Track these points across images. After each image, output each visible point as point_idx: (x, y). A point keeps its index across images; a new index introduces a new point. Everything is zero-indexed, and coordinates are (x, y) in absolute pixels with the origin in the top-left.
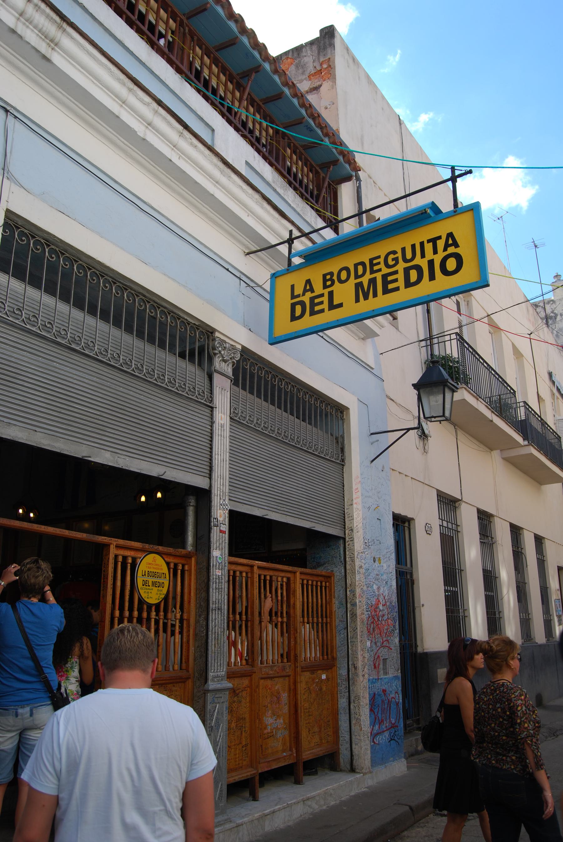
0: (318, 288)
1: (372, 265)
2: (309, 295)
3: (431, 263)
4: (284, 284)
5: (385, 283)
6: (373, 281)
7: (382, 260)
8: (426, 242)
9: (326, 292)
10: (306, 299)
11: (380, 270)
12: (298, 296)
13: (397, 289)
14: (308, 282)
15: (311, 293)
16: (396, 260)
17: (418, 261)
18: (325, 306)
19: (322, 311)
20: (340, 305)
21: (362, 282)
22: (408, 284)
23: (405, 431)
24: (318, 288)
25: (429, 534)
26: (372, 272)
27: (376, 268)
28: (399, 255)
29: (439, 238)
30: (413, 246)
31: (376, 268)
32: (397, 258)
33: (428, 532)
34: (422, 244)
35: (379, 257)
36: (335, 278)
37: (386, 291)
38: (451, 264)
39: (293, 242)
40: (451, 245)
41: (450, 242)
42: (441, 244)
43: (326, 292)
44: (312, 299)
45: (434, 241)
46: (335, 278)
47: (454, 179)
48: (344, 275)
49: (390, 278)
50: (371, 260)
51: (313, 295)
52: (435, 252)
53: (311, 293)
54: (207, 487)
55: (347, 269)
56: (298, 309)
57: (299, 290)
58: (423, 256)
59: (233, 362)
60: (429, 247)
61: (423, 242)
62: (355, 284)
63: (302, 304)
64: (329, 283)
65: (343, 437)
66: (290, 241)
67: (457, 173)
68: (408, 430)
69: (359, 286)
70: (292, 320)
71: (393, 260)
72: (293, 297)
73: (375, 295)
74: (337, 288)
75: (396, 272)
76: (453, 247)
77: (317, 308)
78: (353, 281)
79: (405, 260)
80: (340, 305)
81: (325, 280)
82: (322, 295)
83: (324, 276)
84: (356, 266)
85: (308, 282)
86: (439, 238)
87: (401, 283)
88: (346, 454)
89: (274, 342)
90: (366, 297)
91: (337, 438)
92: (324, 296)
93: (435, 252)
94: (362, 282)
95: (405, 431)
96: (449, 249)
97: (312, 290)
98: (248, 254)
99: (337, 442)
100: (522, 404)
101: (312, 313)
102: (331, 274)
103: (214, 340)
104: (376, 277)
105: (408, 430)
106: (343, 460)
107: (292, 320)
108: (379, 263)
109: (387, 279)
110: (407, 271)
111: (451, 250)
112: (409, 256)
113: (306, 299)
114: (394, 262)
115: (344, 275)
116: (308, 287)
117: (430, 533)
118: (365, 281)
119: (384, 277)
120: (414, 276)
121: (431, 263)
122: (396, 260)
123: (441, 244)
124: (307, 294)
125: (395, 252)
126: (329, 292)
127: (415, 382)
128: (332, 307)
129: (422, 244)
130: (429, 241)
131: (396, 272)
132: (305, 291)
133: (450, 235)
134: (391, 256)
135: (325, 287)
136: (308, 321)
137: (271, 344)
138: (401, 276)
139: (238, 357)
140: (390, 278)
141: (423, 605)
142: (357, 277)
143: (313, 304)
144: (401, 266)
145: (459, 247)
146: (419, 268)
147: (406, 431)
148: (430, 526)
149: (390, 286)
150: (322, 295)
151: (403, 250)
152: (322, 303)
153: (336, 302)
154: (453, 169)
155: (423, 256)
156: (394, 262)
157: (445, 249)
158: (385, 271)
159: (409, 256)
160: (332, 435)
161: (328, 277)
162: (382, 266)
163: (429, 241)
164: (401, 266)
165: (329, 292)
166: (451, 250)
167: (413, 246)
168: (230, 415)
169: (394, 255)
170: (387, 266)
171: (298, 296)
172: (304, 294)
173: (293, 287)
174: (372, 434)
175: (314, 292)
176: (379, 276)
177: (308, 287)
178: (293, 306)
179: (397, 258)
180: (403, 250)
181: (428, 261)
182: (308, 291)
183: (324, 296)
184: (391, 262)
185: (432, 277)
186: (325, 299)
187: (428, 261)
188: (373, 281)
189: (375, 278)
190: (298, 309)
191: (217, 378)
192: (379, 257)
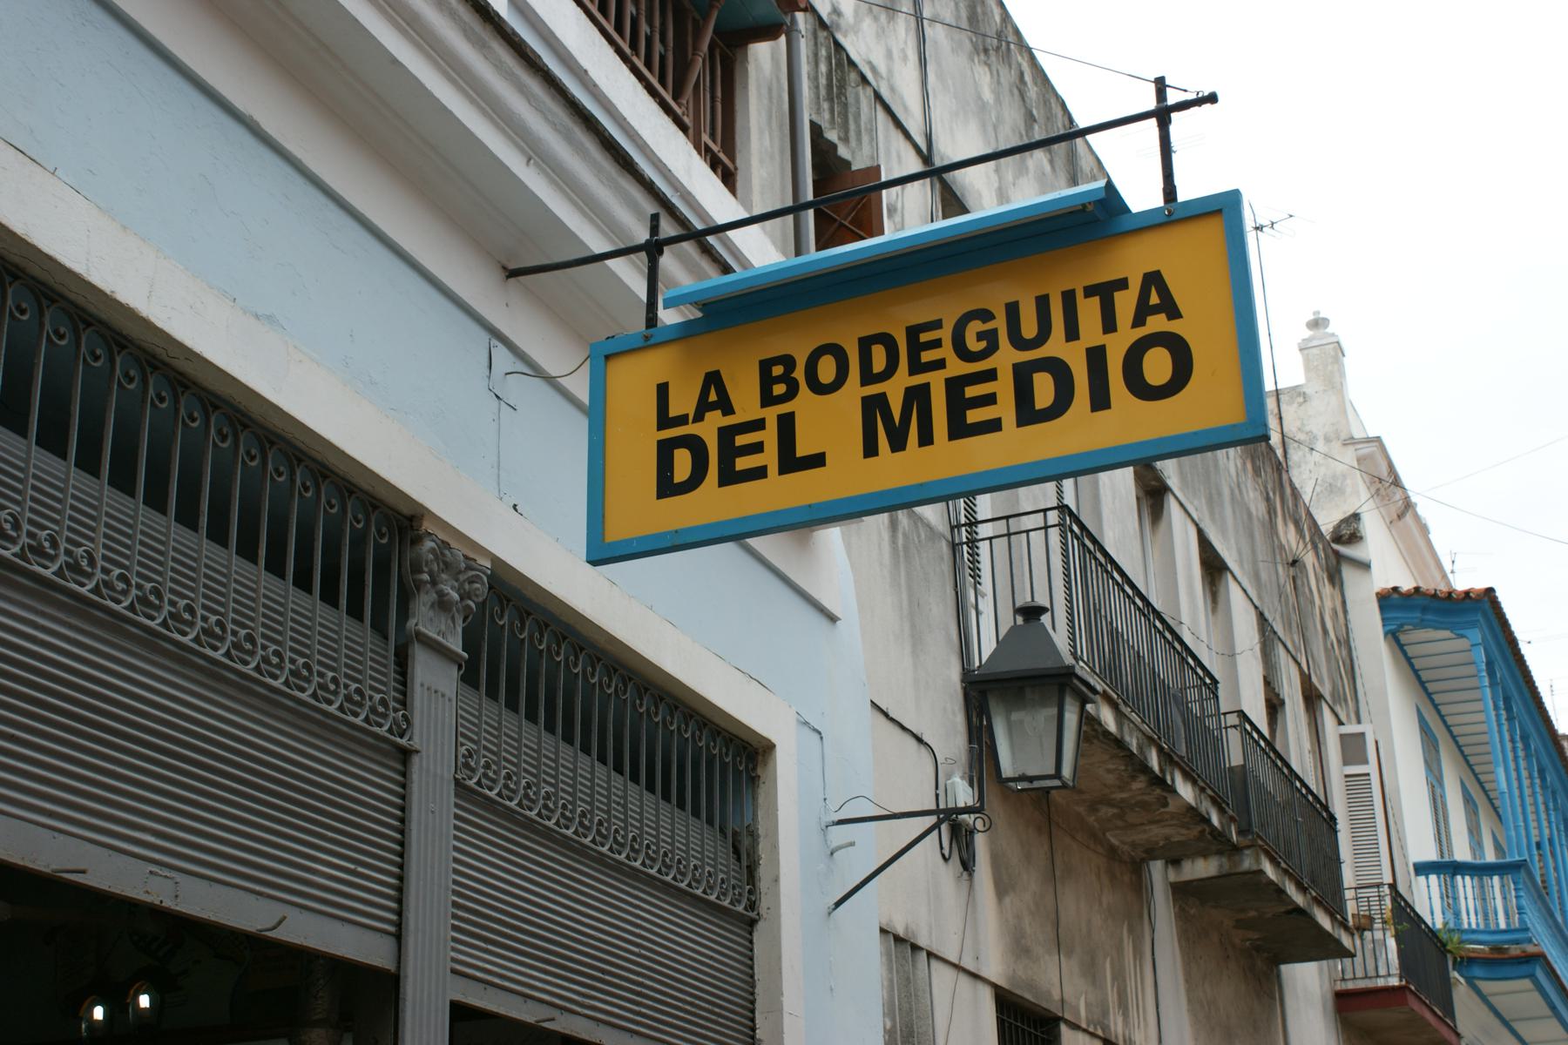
0: (747, 403)
1: (915, 347)
2: (715, 420)
3: (1096, 357)
5: (958, 404)
6: (918, 397)
7: (945, 334)
8: (1080, 294)
9: (771, 415)
10: (708, 429)
11: (940, 364)
12: (682, 420)
13: (994, 426)
14: (713, 379)
15: (725, 414)
16: (990, 337)
17: (1056, 346)
18: (770, 458)
19: (760, 473)
20: (817, 460)
21: (883, 395)
22: (1028, 414)
24: (747, 403)
26: (916, 367)
27: (927, 356)
28: (1000, 324)
29: (1122, 284)
31: (927, 356)
32: (995, 331)
34: (1069, 298)
35: (937, 325)
36: (799, 374)
37: (959, 429)
38: (1158, 366)
39: (661, 252)
40: (1156, 310)
41: (1154, 299)
42: (1125, 303)
43: (771, 415)
44: (726, 435)
45: (1105, 292)
46: (799, 374)
47: (1163, 115)
48: (827, 370)
49: (971, 392)
50: (913, 332)
52: (1109, 325)
53: (725, 414)
56: (683, 463)
58: (1072, 333)
59: (468, 607)
60: (1090, 311)
61: (1073, 291)
63: (696, 446)
64: (779, 389)
65: (753, 834)
66: (654, 249)
67: (1173, 98)
69: (874, 407)
70: (661, 494)
72: (664, 421)
73: (926, 439)
74: (805, 405)
75: (991, 375)
76: (1163, 316)
77: (742, 463)
78: (854, 391)
79: (1019, 342)
80: (817, 460)
81: (767, 381)
82: (759, 425)
83: (765, 366)
84: (865, 344)
85: (713, 379)
86: (1122, 284)
87: (1005, 408)
89: (601, 555)
90: (898, 444)
92: (763, 428)
93: (1109, 325)
94: (883, 395)
96: (1150, 319)
97: (726, 407)
98: (513, 274)
99: (737, 851)
100: (1233, 720)
101: (729, 477)
102: (788, 362)
103: (417, 540)
106: (752, 906)
107: (661, 494)
108: (937, 344)
109: (963, 392)
111: (1157, 323)
112: (1029, 329)
113: (708, 429)
114: (983, 344)
115: (827, 370)
116: (713, 397)
118: (895, 390)
119: (955, 386)
120: (1044, 390)
121: (1096, 357)
122: (990, 337)
123: (1125, 303)
124: (708, 415)
125: (986, 315)
126: (780, 417)
128: (791, 462)
129: (1069, 298)
130: (1090, 291)
131: (991, 375)
132: (703, 408)
133: (1154, 280)
134: (975, 327)
135: (767, 400)
137: (594, 563)
138: (1004, 388)
139: (481, 588)
140: (971, 392)
142: (868, 378)
143: (729, 451)
144: (1006, 358)
146: (1059, 370)
150: (759, 425)
151: (1013, 311)
152: (758, 448)
153: (801, 451)
154: (1161, 85)
155: (1072, 333)
156: (983, 344)
157: (1139, 321)
158: (957, 367)
159: (1029, 329)
161: (778, 370)
162: (947, 352)
163: (1090, 291)
164: (1006, 358)
165: (780, 417)
166: (1157, 323)
167: (1043, 303)
168: (456, 772)
169: (984, 322)
170: (964, 354)
171: (682, 420)
172: (699, 417)
173: (663, 391)
175: (733, 412)
176: (936, 382)
177: (713, 397)
178: (665, 451)
179: (995, 331)
182: (713, 407)
183: (763, 428)
184: (974, 345)
185: (1100, 400)
186: (770, 437)
188: (918, 397)
189: (926, 388)
190: (683, 463)
192: (937, 325)
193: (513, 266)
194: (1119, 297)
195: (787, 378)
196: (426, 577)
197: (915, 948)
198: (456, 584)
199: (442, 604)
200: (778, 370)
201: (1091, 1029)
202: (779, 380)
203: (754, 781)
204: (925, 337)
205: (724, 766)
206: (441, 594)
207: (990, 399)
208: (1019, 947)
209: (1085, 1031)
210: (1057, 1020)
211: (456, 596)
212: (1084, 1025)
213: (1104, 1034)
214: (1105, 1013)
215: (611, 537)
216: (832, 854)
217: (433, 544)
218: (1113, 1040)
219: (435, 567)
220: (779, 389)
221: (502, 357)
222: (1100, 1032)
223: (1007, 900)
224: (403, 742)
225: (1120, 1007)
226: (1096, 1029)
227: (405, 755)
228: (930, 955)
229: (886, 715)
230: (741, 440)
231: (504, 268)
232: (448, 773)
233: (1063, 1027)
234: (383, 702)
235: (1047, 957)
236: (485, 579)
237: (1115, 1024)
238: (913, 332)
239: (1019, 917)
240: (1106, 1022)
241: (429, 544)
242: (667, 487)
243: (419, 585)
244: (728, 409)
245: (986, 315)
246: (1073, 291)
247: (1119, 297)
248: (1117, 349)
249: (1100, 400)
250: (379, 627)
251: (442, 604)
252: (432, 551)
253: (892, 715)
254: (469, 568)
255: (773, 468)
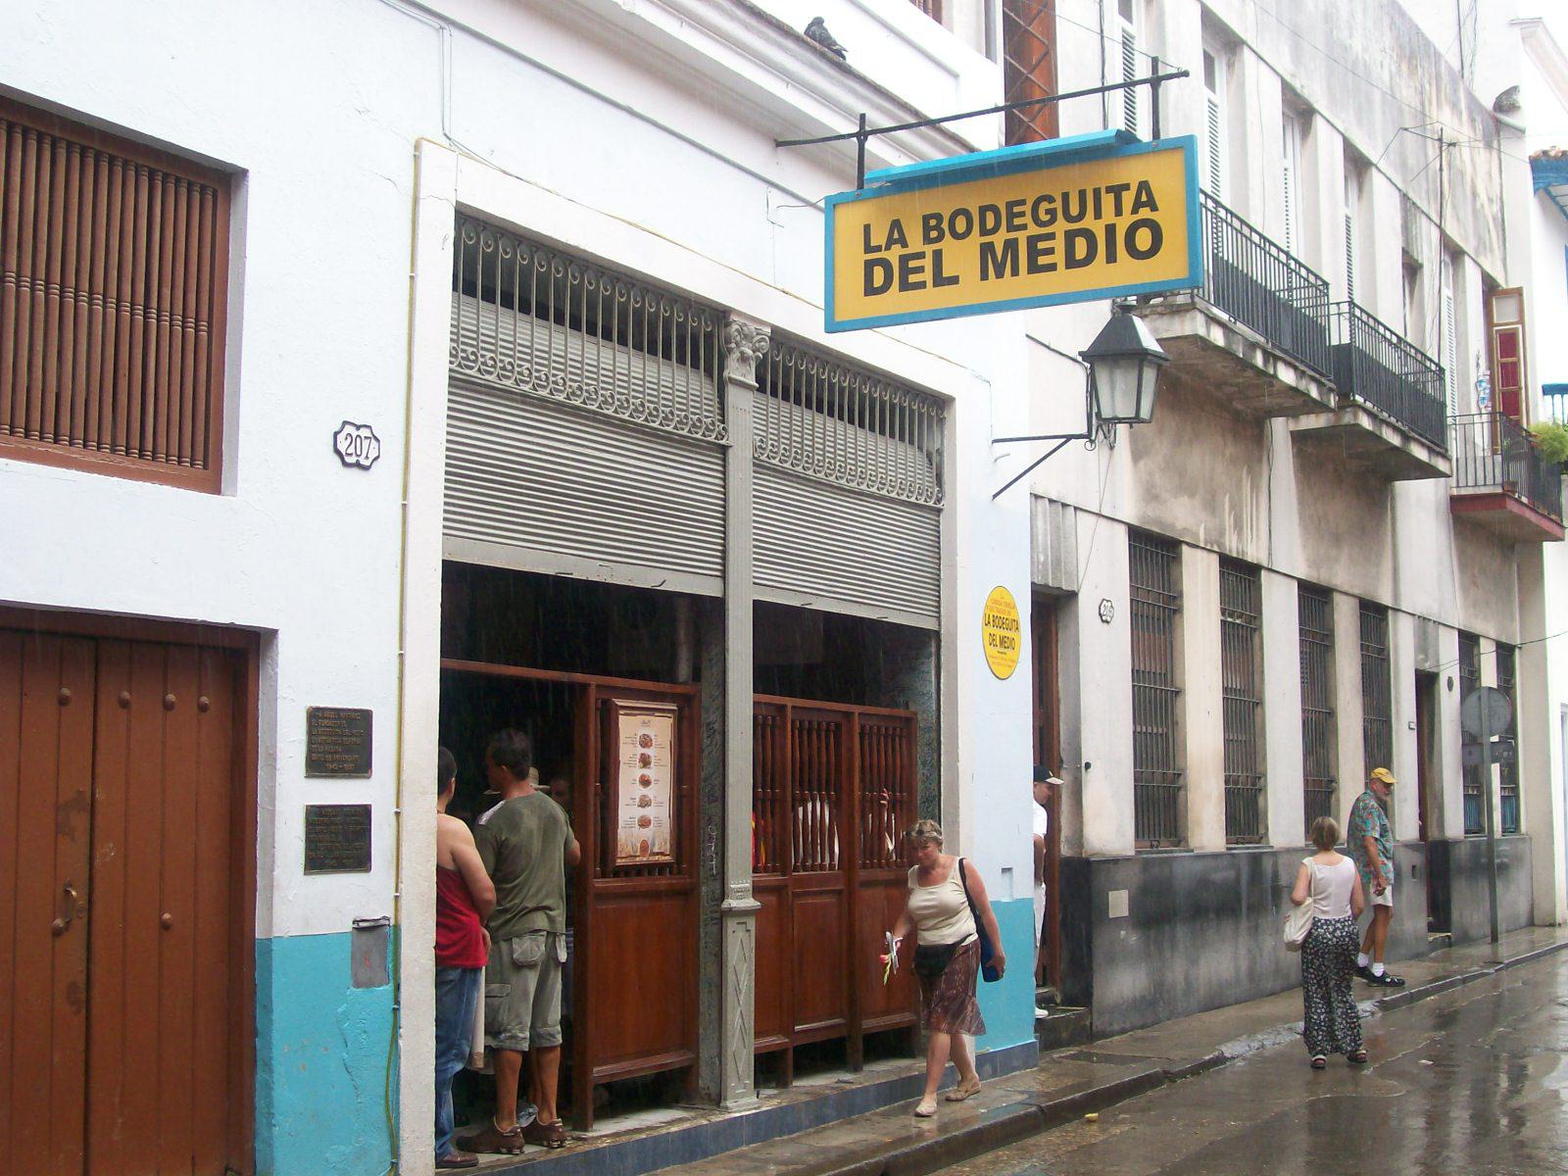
0: (915, 243)
1: (1011, 216)
3: (1111, 230)
4: (852, 219)
5: (1033, 253)
6: (1011, 246)
7: (1027, 208)
8: (1103, 191)
9: (929, 249)
11: (1024, 227)
12: (878, 249)
13: (1052, 267)
14: (896, 225)
15: (903, 247)
16: (1052, 212)
17: (1088, 222)
18: (927, 276)
19: (922, 285)
20: (954, 280)
22: (1071, 262)
23: (1064, 440)
24: (915, 243)
25: (1107, 622)
26: (1011, 228)
27: (1017, 221)
28: (1058, 205)
29: (1126, 187)
30: (1082, 194)
31: (1017, 221)
32: (1055, 209)
33: (1104, 618)
34: (1097, 193)
35: (1022, 202)
36: (945, 226)
37: (1034, 268)
38: (1143, 240)
39: (866, 139)
40: (1144, 205)
41: (1144, 198)
42: (1128, 198)
44: (904, 260)
45: (1117, 191)
46: (945, 226)
48: (961, 225)
49: (1041, 245)
50: (1010, 205)
51: (905, 251)
52: (1119, 212)
53: (903, 247)
54: (719, 595)
55: (966, 213)
56: (879, 274)
57: (879, 238)
58: (1098, 215)
59: (758, 357)
60: (1108, 201)
61: (1099, 189)
62: (981, 244)
63: (886, 265)
64: (934, 234)
65: (940, 453)
68: (1069, 438)
69: (987, 249)
71: (1047, 212)
72: (868, 249)
73: (1015, 272)
74: (948, 244)
75: (1051, 236)
76: (1148, 209)
77: (913, 278)
78: (976, 239)
79: (1068, 218)
80: (954, 280)
81: (927, 229)
82: (921, 255)
83: (926, 219)
84: (983, 210)
85: (896, 225)
86: (1126, 187)
87: (1059, 257)
88: (947, 487)
89: (832, 327)
90: (999, 274)
91: (929, 456)
93: (1119, 212)
95: (1064, 440)
97: (905, 245)
98: (779, 144)
99: (930, 461)
101: (905, 286)
102: (939, 217)
103: (728, 325)
104: (1017, 239)
105: (1069, 438)
108: (1022, 214)
110: (1070, 237)
111: (1145, 213)
112: (1074, 211)
113: (893, 255)
114: (1048, 217)
115: (961, 225)
116: (896, 236)
117: (1109, 619)
118: (999, 240)
119: (1032, 241)
120: (1081, 248)
121: (1111, 230)
122: (1052, 212)
123: (1128, 198)
125: (1050, 199)
127: (1085, 349)
128: (940, 280)
129: (1097, 193)
130: (1109, 190)
133: (1144, 186)
134: (1044, 206)
135: (927, 240)
136: (894, 300)
138: (1059, 244)
139: (765, 345)
140: (1041, 245)
141: (1088, 766)
142: (984, 232)
143: (905, 271)
144: (1061, 226)
145: (1157, 210)
146: (1089, 236)
147: (1064, 440)
148: (1109, 604)
149: (1042, 260)
150: (921, 255)
151: (1066, 197)
156: (1048, 217)
157: (1135, 211)
158: (1034, 230)
159: (1074, 211)
160: (920, 449)
161: (933, 222)
162: (1028, 219)
163: (1109, 190)
164: (1061, 226)
166: (1145, 213)
167: (1082, 194)
171: (878, 249)
172: (888, 248)
173: (867, 228)
174: (996, 441)
176: (1022, 237)
177: (896, 236)
178: (869, 266)
179: (1055, 209)
180: (1066, 197)
181: (1107, 226)
182: (896, 242)
185: (1111, 257)
186: (928, 263)
187: (1107, 226)
188: (1011, 246)
190: (879, 274)
191: (732, 393)
192: (1022, 202)
193: (780, 140)
194: (1124, 194)
195: (938, 228)
196: (733, 345)
197: (1064, 505)
198: (751, 345)
199: (744, 359)
200: (933, 222)
201: (1208, 547)
202: (934, 228)
203: (941, 421)
204: (1016, 209)
205: (921, 415)
206: (742, 353)
207: (1050, 251)
208: (1150, 495)
209: (1203, 548)
210: (1182, 542)
211: (750, 352)
212: (1202, 545)
213: (1219, 548)
214: (1222, 534)
215: (838, 319)
216: (996, 460)
217: (737, 327)
218: (1227, 552)
219: (738, 338)
220: (934, 234)
221: (777, 197)
222: (1216, 549)
223: (1142, 464)
224: (723, 442)
225: (1235, 527)
226: (1212, 546)
227: (724, 450)
228: (1076, 508)
229: (1048, 347)
230: (912, 264)
231: (775, 140)
232: (749, 453)
233: (1185, 548)
234: (713, 424)
235: (1173, 499)
236: (767, 339)
237: (1230, 541)
238: (1010, 205)
239: (1150, 474)
240: (1222, 541)
241: (735, 327)
242: (870, 290)
243: (730, 351)
244: (905, 245)
245: (1050, 199)
246: (1099, 189)
247: (1124, 194)
248: (1122, 226)
249: (1111, 257)
250: (709, 373)
251: (744, 359)
252: (737, 330)
253: (1052, 347)
254: (758, 334)
255: (930, 283)
